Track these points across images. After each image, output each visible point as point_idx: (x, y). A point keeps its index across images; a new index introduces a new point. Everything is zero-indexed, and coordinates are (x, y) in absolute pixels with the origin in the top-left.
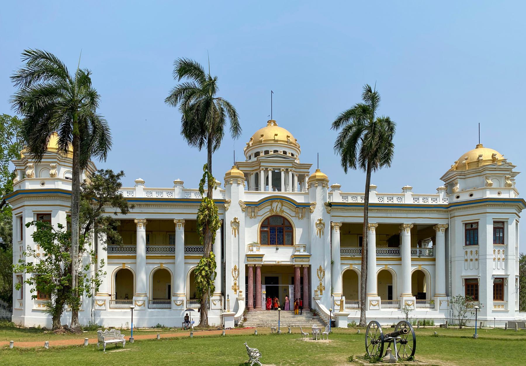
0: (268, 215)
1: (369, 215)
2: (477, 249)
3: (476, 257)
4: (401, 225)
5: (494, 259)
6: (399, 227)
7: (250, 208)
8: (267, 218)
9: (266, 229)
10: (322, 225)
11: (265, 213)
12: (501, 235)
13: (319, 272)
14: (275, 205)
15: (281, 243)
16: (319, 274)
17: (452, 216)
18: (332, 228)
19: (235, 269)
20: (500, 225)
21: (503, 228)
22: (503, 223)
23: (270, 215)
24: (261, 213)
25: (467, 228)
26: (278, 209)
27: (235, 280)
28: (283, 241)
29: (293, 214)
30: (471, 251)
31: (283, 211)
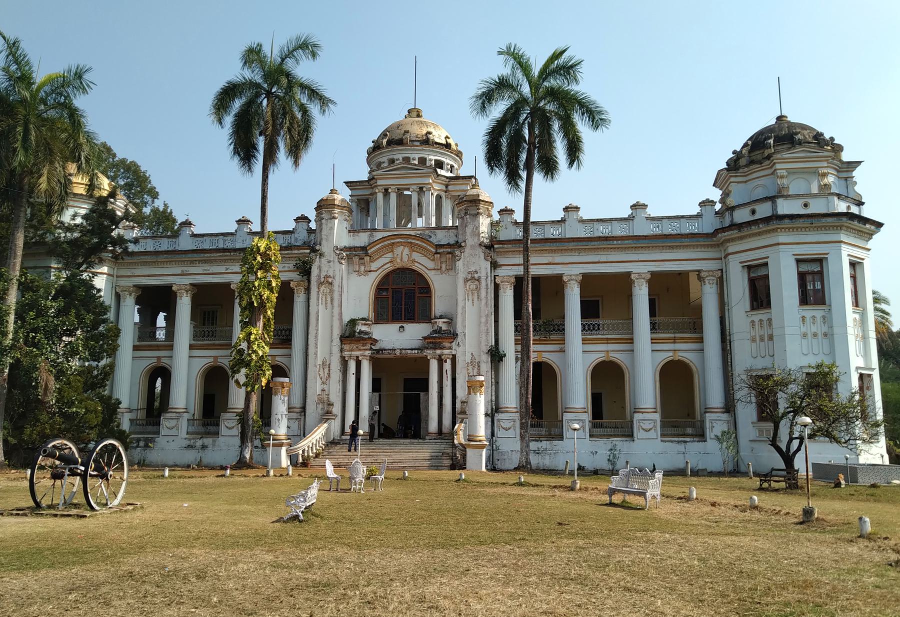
0: (389, 267)
2: (768, 316)
3: (770, 333)
4: (629, 274)
7: (356, 255)
8: (387, 276)
11: (382, 264)
14: (399, 250)
15: (411, 318)
20: (816, 268)
21: (821, 273)
22: (820, 261)
23: (391, 268)
24: (375, 265)
25: (752, 275)
26: (405, 258)
30: (761, 321)
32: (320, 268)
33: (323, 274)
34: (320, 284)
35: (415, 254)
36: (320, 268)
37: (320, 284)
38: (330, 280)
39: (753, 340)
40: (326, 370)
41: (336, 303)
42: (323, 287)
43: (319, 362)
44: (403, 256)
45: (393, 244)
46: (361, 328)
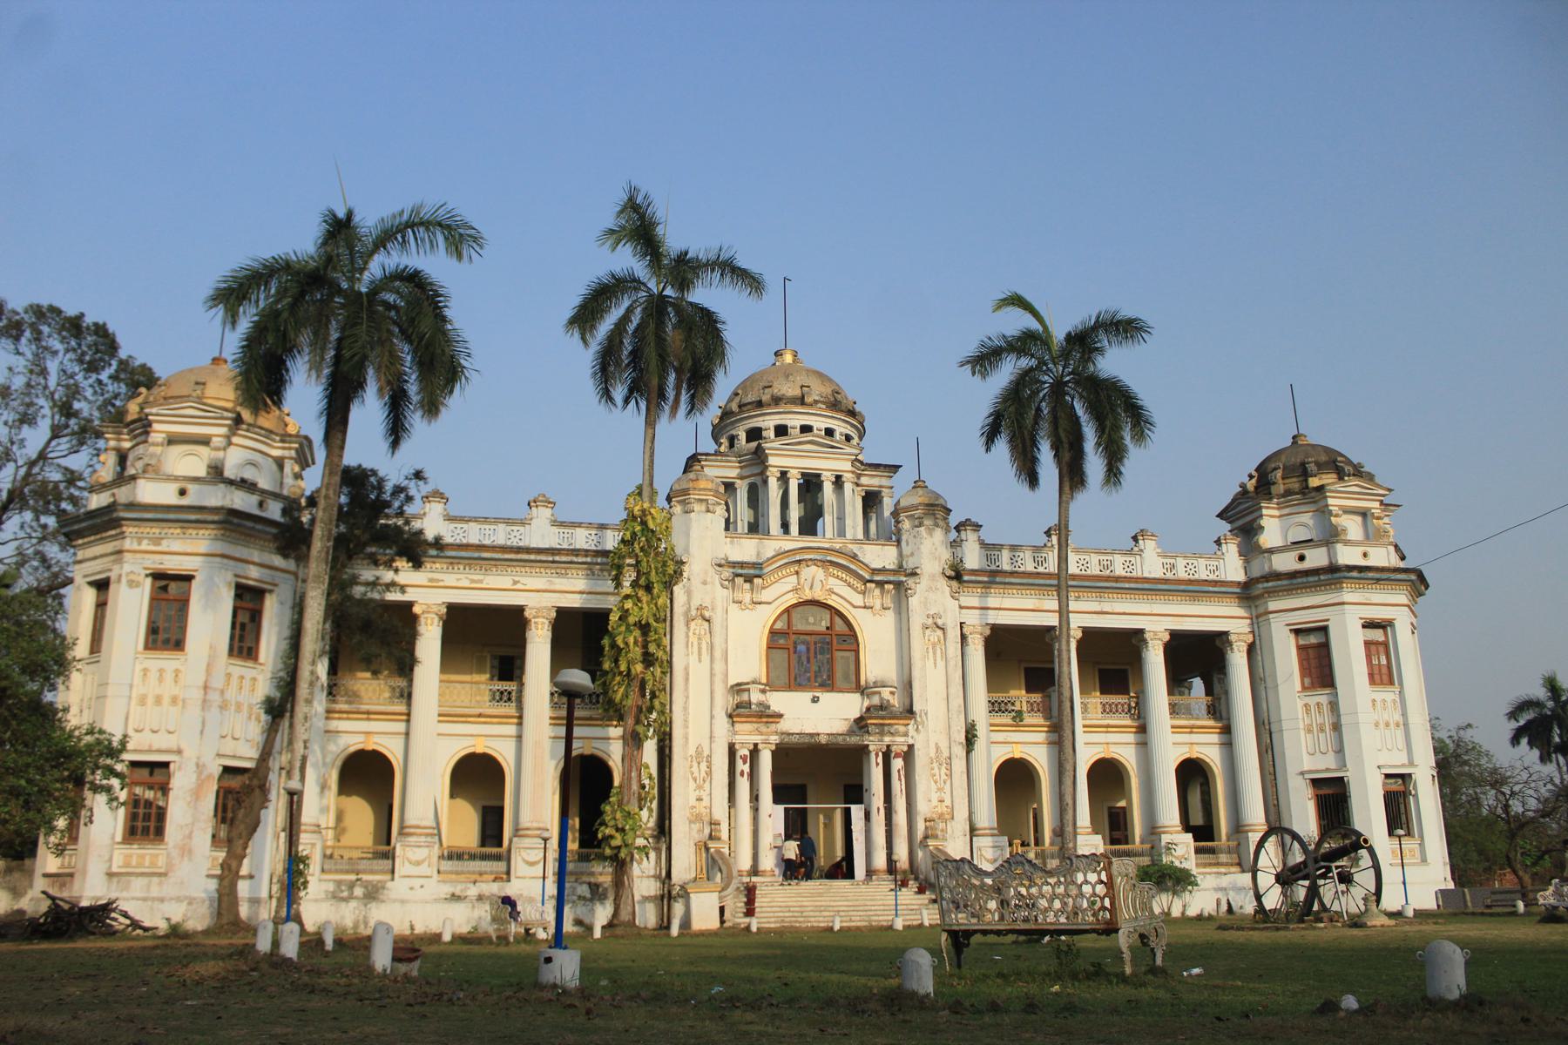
1: (1073, 605)
4: (1140, 632)
5: (1377, 725)
6: (1132, 641)
9: (782, 641)
10: (940, 633)
12: (1384, 661)
13: (935, 765)
16: (936, 771)
17: (1261, 610)
18: (963, 637)
19: (699, 752)
27: (699, 787)
28: (831, 676)
29: (858, 599)
31: (831, 591)
32: (689, 593)
33: (695, 603)
34: (689, 621)
35: (832, 581)
36: (689, 593)
37: (689, 621)
38: (707, 614)
39: (1310, 731)
40: (704, 766)
41: (718, 654)
42: (693, 625)
43: (692, 751)
44: (820, 583)
45: (799, 561)
46: (756, 697)
